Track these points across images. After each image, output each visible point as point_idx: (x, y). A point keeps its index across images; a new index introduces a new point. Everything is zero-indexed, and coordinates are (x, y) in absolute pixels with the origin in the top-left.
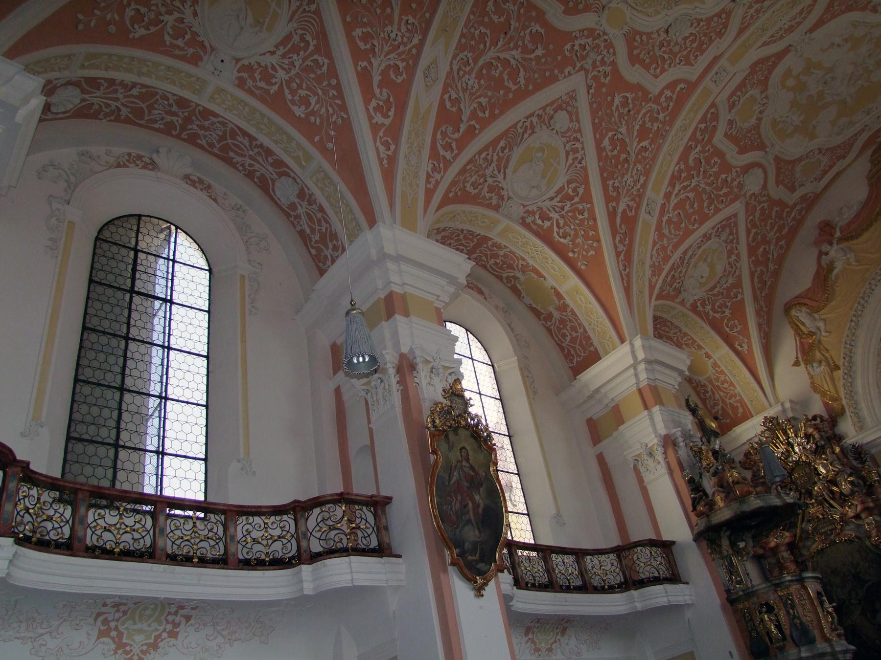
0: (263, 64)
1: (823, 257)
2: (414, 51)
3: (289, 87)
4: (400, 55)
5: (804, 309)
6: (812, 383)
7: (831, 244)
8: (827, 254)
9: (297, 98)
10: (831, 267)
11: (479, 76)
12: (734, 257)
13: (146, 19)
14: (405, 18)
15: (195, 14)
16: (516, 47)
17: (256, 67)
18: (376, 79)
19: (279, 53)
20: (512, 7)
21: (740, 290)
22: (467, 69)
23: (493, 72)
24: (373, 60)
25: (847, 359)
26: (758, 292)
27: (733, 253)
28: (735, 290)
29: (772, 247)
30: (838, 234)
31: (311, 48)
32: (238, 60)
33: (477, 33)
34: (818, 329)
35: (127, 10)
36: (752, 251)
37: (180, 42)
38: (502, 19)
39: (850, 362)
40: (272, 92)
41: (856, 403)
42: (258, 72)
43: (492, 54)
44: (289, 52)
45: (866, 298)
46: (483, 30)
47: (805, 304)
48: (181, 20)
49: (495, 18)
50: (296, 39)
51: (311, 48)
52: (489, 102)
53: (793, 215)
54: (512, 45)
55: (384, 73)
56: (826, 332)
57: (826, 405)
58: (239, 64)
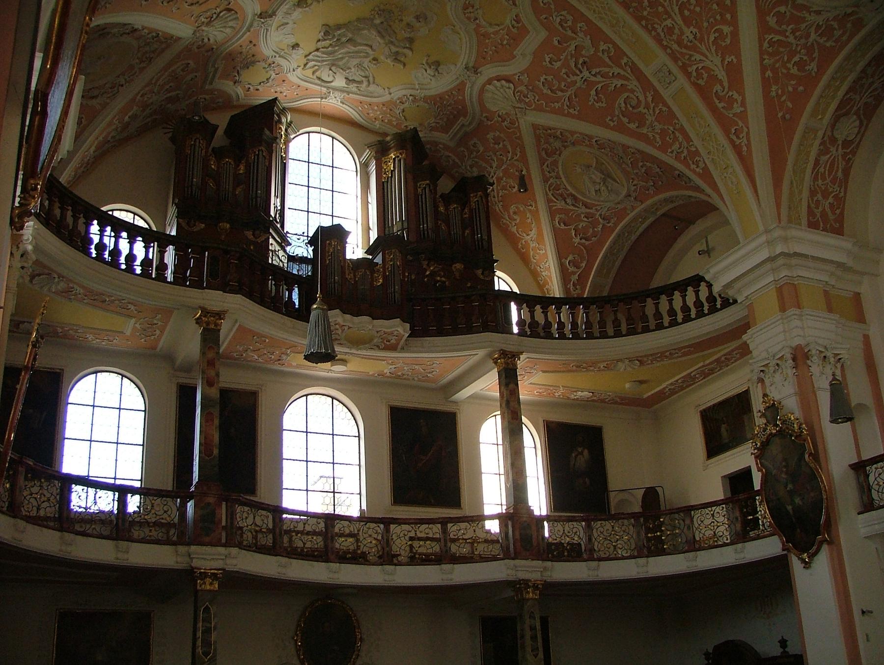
13: (805, 58)
15: (818, 13)
35: (792, 71)
37: (837, 33)
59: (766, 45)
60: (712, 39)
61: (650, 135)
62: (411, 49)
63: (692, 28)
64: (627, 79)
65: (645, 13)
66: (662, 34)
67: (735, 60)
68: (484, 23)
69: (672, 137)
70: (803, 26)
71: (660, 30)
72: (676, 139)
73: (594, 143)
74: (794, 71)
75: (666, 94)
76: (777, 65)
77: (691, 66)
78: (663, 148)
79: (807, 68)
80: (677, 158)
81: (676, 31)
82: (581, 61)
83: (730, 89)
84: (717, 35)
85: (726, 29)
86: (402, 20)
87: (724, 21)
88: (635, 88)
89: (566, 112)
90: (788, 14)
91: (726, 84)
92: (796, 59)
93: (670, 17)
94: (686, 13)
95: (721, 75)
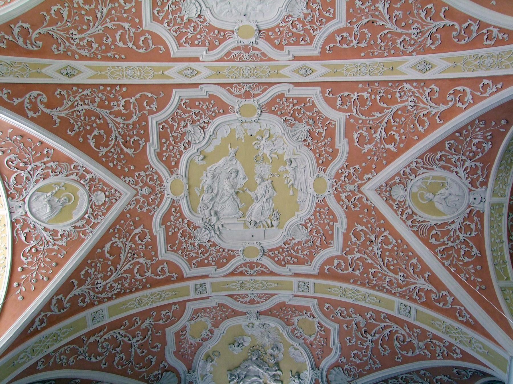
0: (466, 176)
2: (415, 84)
3: (474, 156)
4: (421, 94)
9: (479, 150)
11: (407, 26)
13: (467, 249)
14: (399, 99)
16: (376, 9)
17: (469, 179)
18: (442, 108)
19: (455, 169)
20: (356, 29)
22: (407, 38)
23: (401, 17)
24: (433, 113)
31: (443, 153)
32: (471, 190)
33: (382, 44)
35: (465, 261)
38: (366, 31)
40: (481, 165)
42: (472, 177)
43: (389, 25)
44: (452, 164)
46: (379, 40)
48: (460, 229)
49: (368, 36)
50: (442, 163)
51: (443, 153)
52: (422, 8)
54: (377, 13)
55: (437, 103)
58: (473, 189)
59: (440, 255)
60: (412, 271)
61: (422, 353)
62: (279, 370)
63: (400, 274)
64: (390, 326)
65: (374, 282)
66: (389, 288)
67: (429, 274)
68: (307, 336)
69: (432, 345)
70: (451, 233)
71: (387, 287)
72: (435, 345)
73: (401, 381)
74: (466, 260)
75: (411, 320)
76: (454, 262)
77: (413, 294)
78: (433, 357)
79: (473, 254)
80: (444, 358)
81: (394, 281)
82: (363, 331)
83: (439, 292)
84: (412, 268)
85: (414, 261)
86: (266, 354)
87: (410, 258)
88: (397, 329)
89: (374, 368)
90: (438, 233)
91: (434, 290)
92: (462, 253)
93: (386, 275)
94: (392, 268)
95: (429, 287)
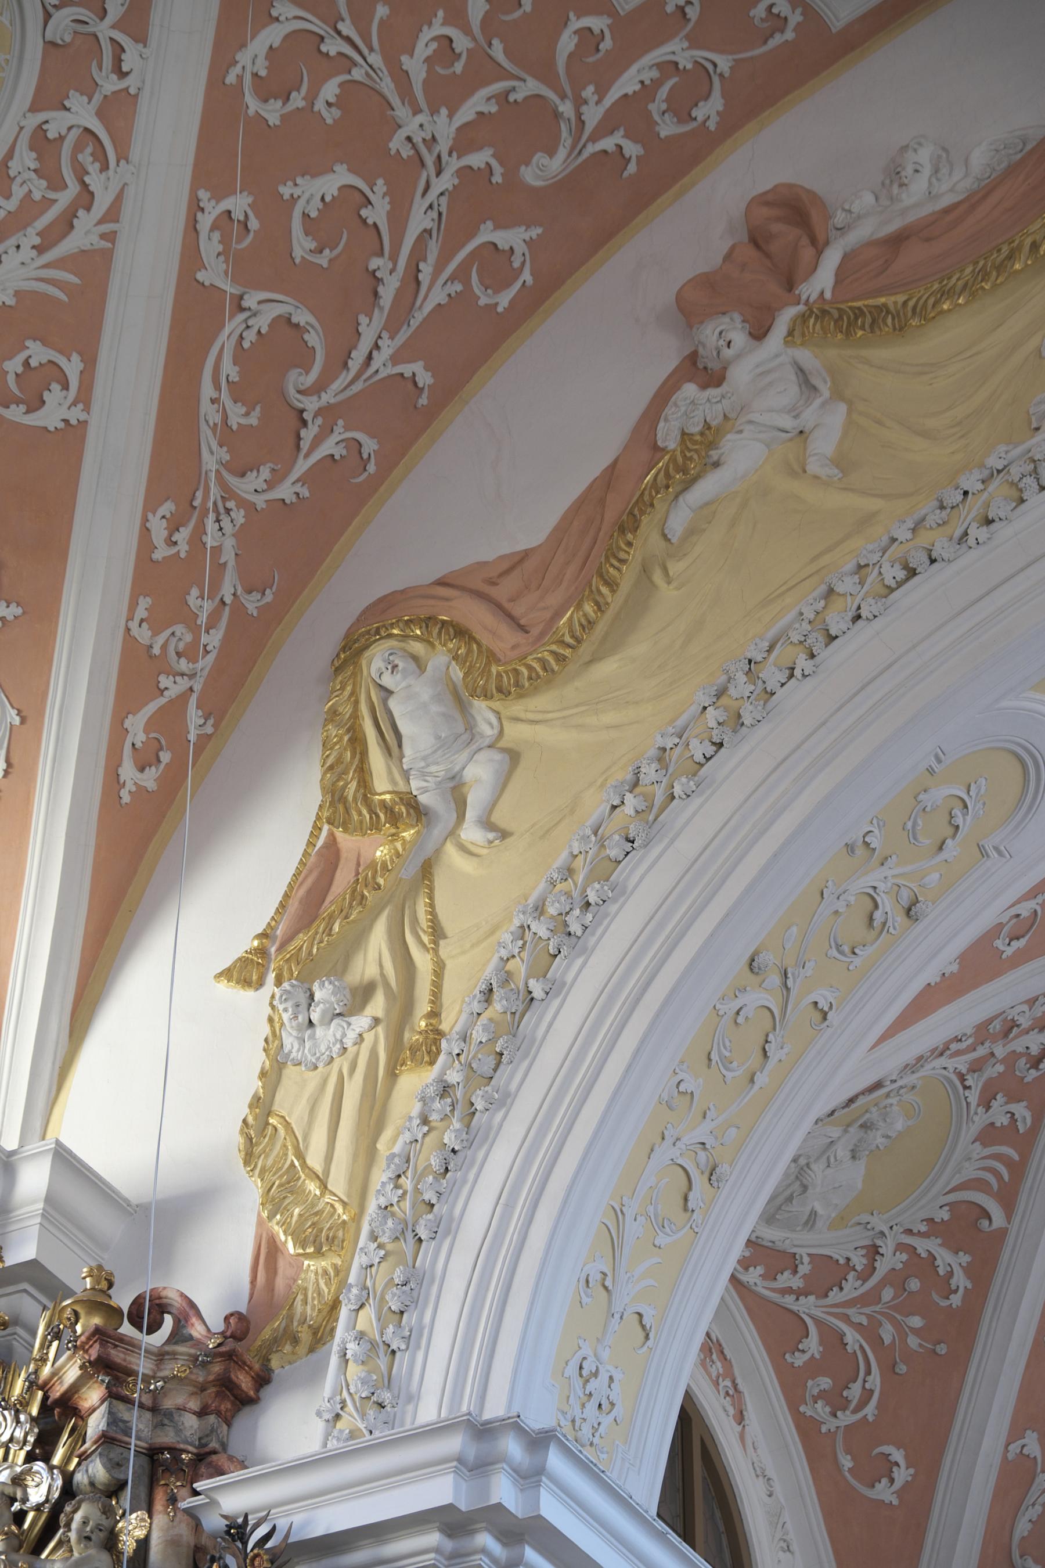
1: (690, 389)
5: (438, 657)
6: (262, 1105)
7: (759, 334)
8: (712, 377)
10: (701, 450)
12: (82, 112)
21: (73, 367)
25: (498, 1005)
26: (212, 457)
27: (89, 88)
28: (38, 353)
29: (419, 220)
30: (821, 282)
34: (456, 792)
36: (228, 145)
39: (512, 1024)
41: (415, 1287)
45: (772, 675)
47: (461, 632)
53: (627, 84)
56: (487, 824)
57: (268, 1254)
